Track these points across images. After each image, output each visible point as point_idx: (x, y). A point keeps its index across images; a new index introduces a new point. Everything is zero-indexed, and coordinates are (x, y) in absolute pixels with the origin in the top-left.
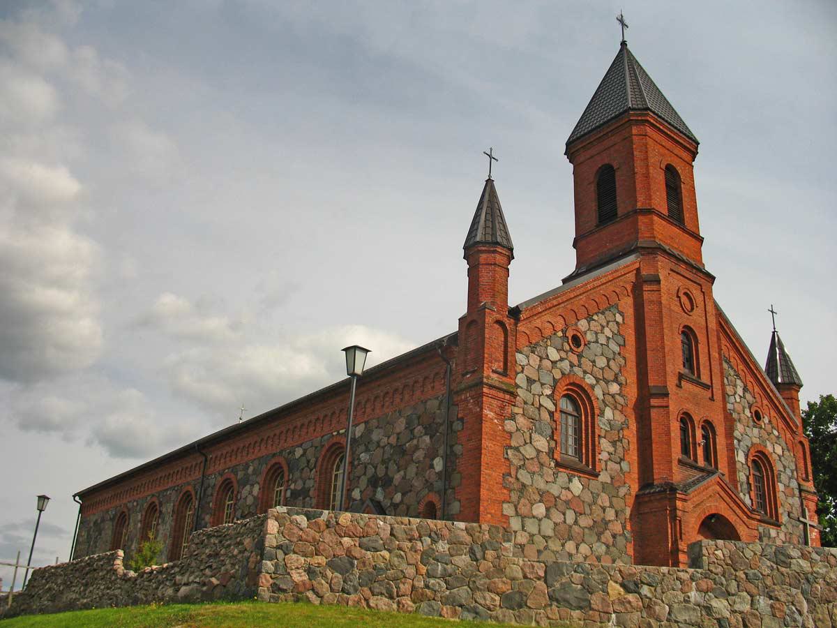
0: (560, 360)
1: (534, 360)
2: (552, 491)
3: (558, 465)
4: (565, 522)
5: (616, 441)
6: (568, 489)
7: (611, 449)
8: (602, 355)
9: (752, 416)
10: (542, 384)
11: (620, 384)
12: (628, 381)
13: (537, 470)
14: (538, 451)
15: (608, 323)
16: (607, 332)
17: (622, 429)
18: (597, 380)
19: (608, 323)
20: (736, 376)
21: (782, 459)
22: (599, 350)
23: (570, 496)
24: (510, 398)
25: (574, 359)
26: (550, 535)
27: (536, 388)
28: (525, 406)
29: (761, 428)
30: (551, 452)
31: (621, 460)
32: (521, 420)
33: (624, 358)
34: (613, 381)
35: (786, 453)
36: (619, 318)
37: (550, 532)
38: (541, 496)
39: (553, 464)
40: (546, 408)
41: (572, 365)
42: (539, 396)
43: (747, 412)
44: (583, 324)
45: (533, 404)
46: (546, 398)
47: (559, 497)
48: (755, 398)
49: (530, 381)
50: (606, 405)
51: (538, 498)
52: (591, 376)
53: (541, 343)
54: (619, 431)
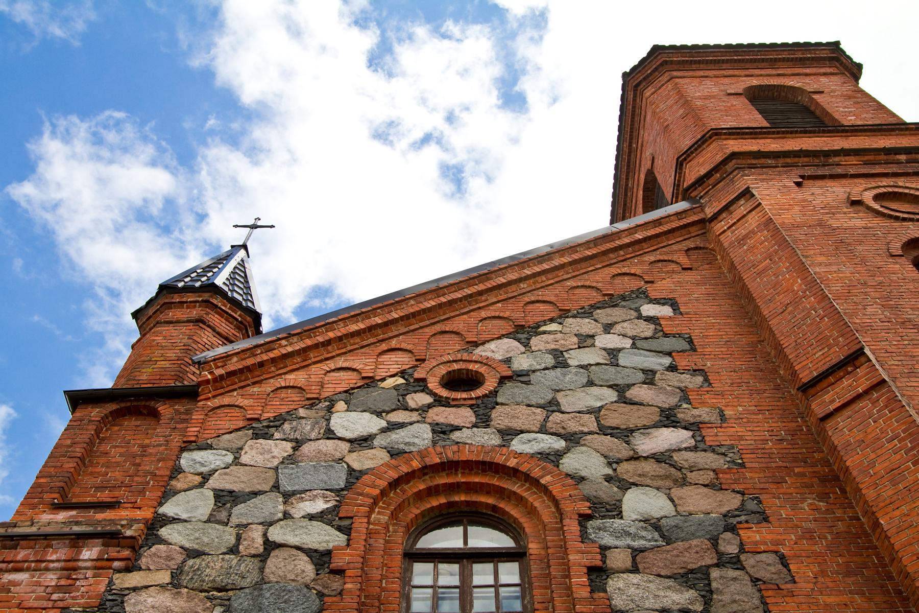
10: (287, 496)
28: (191, 562)
34: (657, 426)
40: (298, 548)
45: (233, 550)
46: (306, 522)
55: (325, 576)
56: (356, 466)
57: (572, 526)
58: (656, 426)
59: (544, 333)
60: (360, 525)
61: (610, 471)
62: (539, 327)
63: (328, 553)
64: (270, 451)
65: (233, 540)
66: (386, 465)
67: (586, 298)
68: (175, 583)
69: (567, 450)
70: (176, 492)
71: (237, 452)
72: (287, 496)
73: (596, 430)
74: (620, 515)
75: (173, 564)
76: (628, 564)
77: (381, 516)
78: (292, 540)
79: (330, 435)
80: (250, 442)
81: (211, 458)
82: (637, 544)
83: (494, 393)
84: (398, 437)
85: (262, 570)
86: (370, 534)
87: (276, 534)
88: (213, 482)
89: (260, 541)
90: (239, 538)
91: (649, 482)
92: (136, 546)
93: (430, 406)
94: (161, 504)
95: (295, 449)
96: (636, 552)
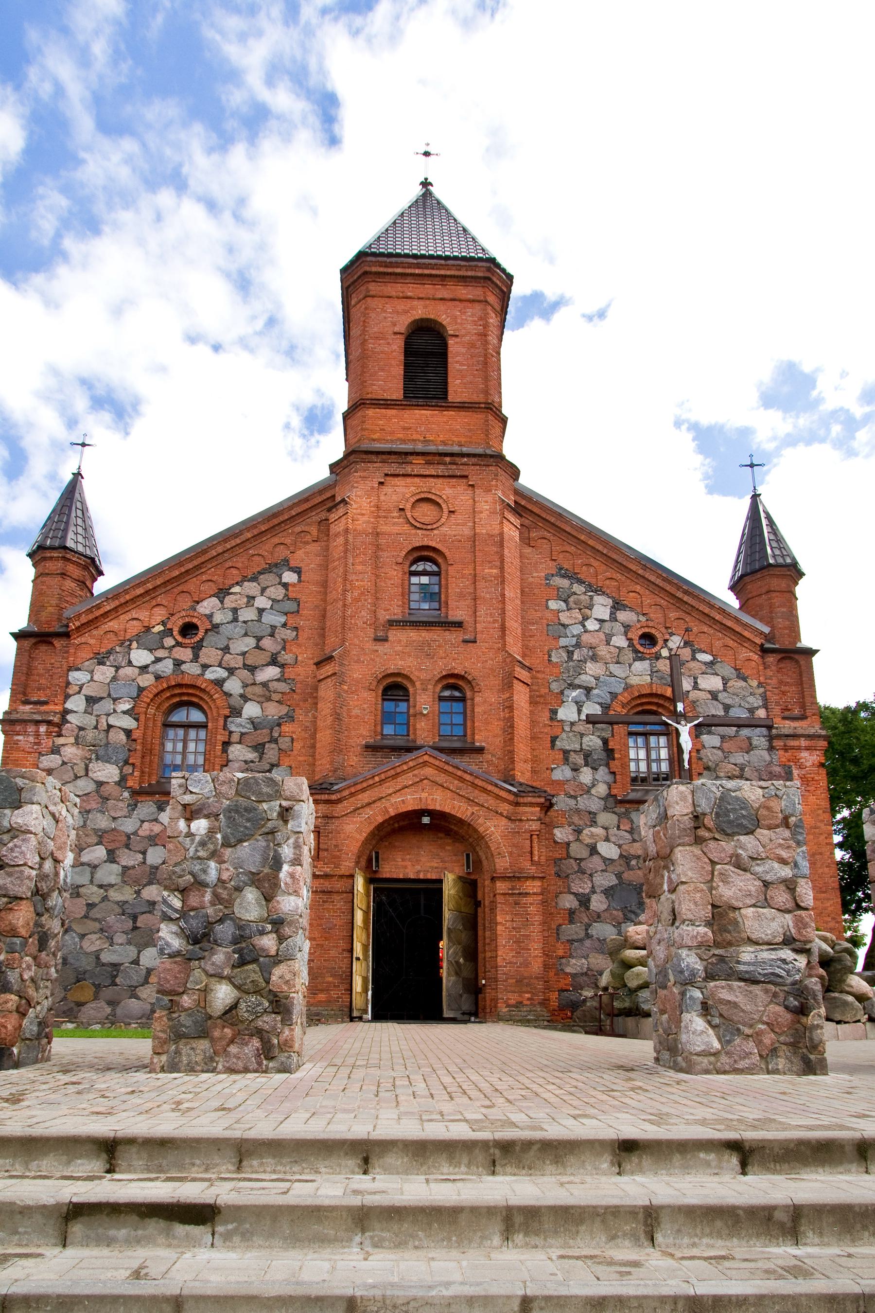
0: (153, 662)
1: (104, 673)
2: (122, 828)
3: (135, 793)
4: (144, 863)
5: (263, 745)
6: (156, 820)
7: (251, 756)
8: (246, 635)
9: (631, 645)
10: (115, 700)
11: (282, 666)
12: (299, 658)
13: (94, 805)
14: (100, 784)
15: (263, 590)
16: (261, 602)
17: (279, 725)
18: (231, 671)
19: (263, 590)
20: (596, 591)
21: (721, 696)
22: (239, 629)
23: (157, 828)
24: (47, 729)
25: (185, 654)
26: (113, 883)
27: (107, 705)
28: (81, 733)
29: (658, 657)
30: (123, 780)
31: (273, 766)
32: (70, 752)
33: (296, 629)
35: (737, 684)
36: (289, 577)
37: (113, 879)
38: (101, 837)
39: (126, 794)
41: (178, 663)
42: (108, 715)
43: (620, 641)
44: (208, 606)
45: (96, 728)
47: (135, 833)
48: (644, 614)
49: (91, 701)
50: (245, 698)
51: (95, 839)
52: (219, 669)
53: (118, 649)
54: (272, 730)
55: (130, 742)
56: (141, 685)
57: (221, 722)
58: (267, 665)
59: (232, 593)
60: (142, 718)
61: (242, 691)
62: (230, 588)
63: (131, 731)
64: (105, 674)
65: (95, 723)
66: (153, 685)
67: (258, 564)
68: (77, 743)
69: (228, 677)
70: (70, 696)
71: (92, 672)
72: (115, 700)
73: (241, 666)
74: (240, 716)
75: (75, 733)
76: (238, 740)
77: (151, 711)
78: (118, 724)
79: (130, 663)
80: (97, 667)
81: (81, 676)
82: (244, 730)
83: (202, 640)
84: (159, 666)
85: (107, 737)
86: (147, 719)
87: (112, 721)
88: (84, 692)
89: (105, 724)
90: (97, 721)
91: (255, 698)
92: (59, 726)
93: (174, 646)
94: (65, 703)
95: (116, 671)
96: (242, 734)
